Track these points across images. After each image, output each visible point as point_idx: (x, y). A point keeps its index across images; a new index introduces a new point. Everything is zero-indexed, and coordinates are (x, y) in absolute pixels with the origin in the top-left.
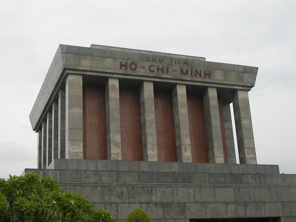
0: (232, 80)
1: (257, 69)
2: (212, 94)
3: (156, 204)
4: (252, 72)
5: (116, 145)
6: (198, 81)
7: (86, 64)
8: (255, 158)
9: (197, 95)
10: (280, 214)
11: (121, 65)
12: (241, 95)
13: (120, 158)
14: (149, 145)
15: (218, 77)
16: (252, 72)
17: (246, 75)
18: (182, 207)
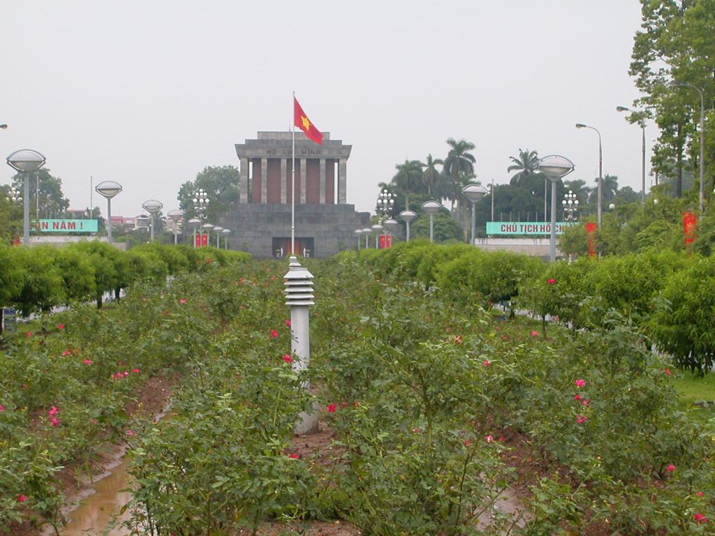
0: (334, 154)
1: (351, 146)
2: (323, 162)
3: (259, 232)
4: (349, 148)
5: (264, 194)
6: (313, 156)
7: (249, 153)
8: (345, 199)
9: (313, 163)
10: (314, 236)
11: (268, 152)
12: (341, 162)
13: (266, 202)
14: (282, 194)
15: (325, 153)
16: (349, 148)
17: (344, 151)
18: (270, 233)
